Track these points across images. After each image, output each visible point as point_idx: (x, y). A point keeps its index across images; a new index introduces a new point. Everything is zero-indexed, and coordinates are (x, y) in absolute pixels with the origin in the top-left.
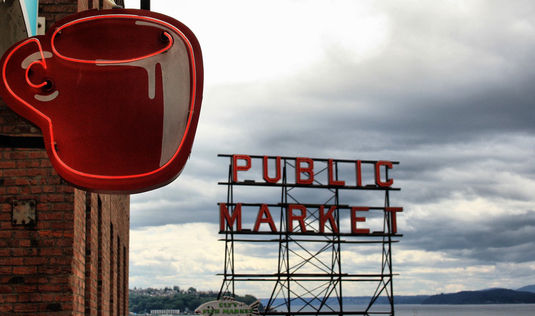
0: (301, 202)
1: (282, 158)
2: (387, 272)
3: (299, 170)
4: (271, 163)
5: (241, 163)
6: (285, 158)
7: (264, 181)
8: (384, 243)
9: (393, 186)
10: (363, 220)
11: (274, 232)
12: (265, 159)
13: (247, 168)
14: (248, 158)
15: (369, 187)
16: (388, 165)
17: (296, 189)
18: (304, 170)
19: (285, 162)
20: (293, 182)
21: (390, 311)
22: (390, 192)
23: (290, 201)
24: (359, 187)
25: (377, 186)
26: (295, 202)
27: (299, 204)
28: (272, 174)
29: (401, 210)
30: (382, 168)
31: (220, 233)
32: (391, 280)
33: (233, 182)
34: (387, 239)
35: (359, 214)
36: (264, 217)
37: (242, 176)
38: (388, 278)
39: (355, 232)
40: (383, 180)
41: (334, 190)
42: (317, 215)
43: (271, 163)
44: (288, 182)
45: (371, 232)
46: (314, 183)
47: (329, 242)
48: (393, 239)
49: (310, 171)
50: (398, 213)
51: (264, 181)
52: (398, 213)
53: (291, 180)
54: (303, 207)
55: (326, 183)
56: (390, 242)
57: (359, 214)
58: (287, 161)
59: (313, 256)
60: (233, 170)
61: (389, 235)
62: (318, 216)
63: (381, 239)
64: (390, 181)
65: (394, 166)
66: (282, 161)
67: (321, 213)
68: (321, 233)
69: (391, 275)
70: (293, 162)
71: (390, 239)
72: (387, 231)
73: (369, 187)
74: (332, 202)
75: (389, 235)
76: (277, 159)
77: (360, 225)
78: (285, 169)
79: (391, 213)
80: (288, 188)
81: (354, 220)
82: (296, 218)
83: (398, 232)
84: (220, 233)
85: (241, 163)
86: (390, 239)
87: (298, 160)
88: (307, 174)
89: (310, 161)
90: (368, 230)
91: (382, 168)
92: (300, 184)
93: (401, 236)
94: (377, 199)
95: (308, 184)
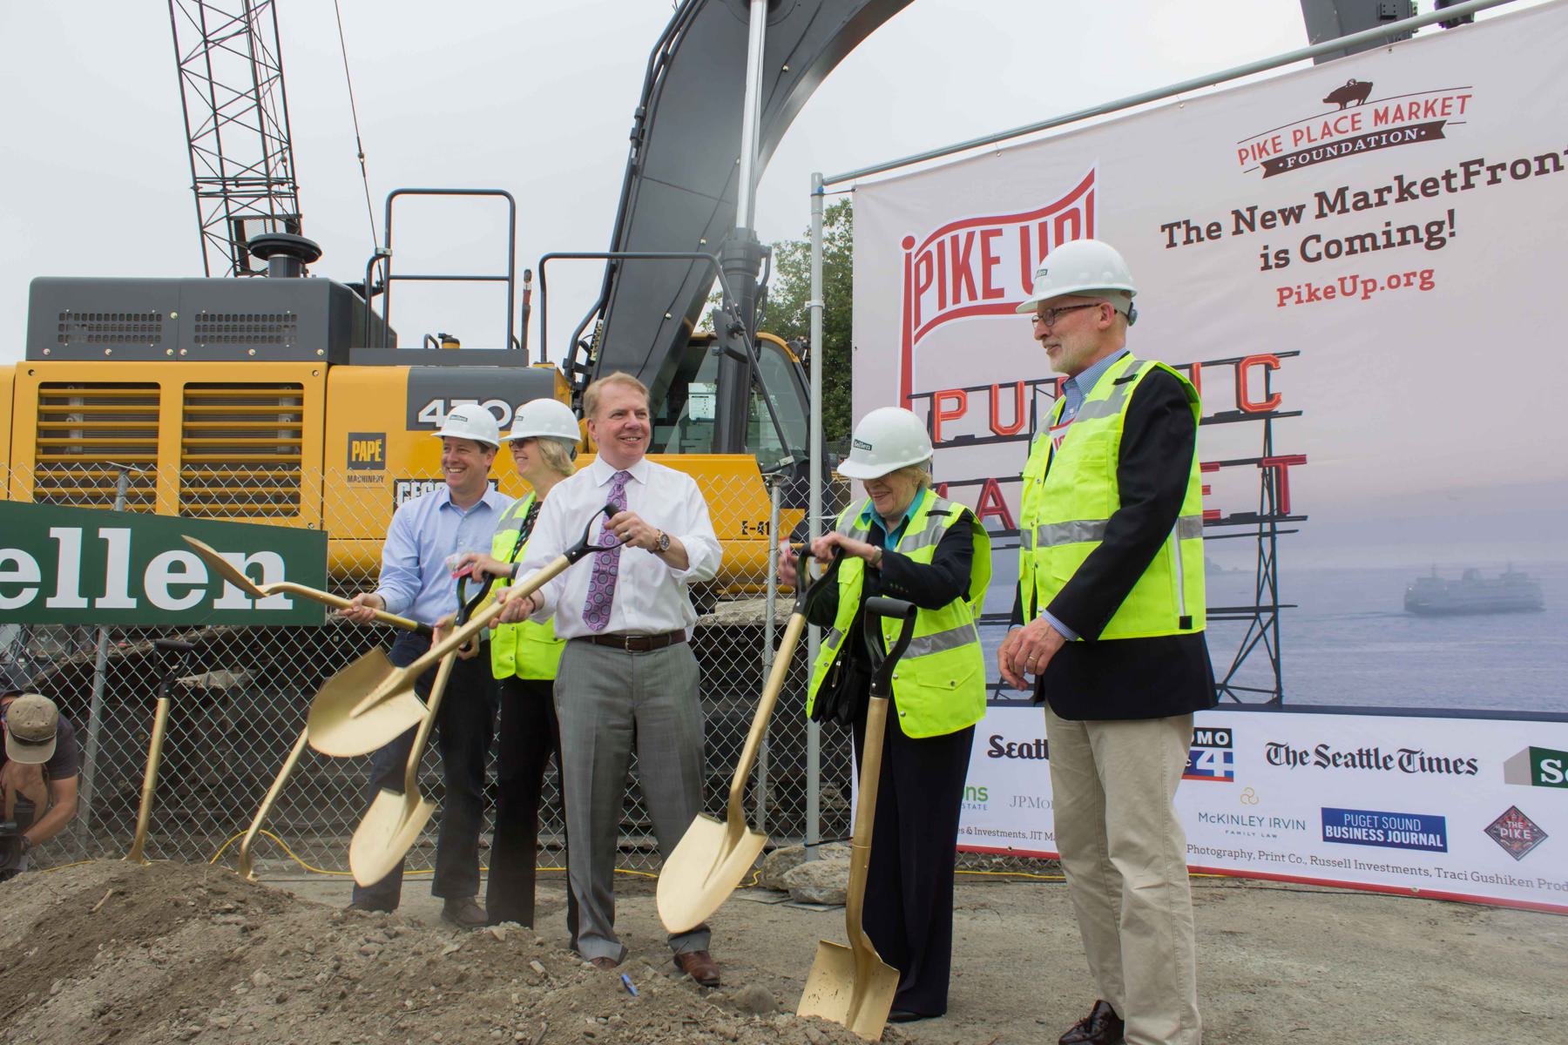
1: (1027, 383)
2: (1266, 600)
4: (1006, 398)
8: (1261, 535)
9: (1280, 409)
14: (961, 394)
16: (1270, 364)
21: (1273, 687)
28: (1006, 419)
29: (1301, 460)
30: (1255, 374)
32: (1275, 619)
34: (1267, 527)
36: (991, 503)
38: (1270, 615)
40: (1256, 396)
43: (1006, 398)
45: (1224, 515)
48: (1280, 526)
50: (1293, 471)
56: (1272, 534)
61: (1272, 519)
63: (1255, 528)
65: (1282, 361)
66: (1028, 390)
69: (1274, 609)
71: (1273, 527)
72: (1266, 511)
73: (1221, 418)
75: (1272, 519)
79: (1275, 469)
86: (1273, 527)
90: (1217, 512)
91: (1255, 374)
93: (1304, 518)
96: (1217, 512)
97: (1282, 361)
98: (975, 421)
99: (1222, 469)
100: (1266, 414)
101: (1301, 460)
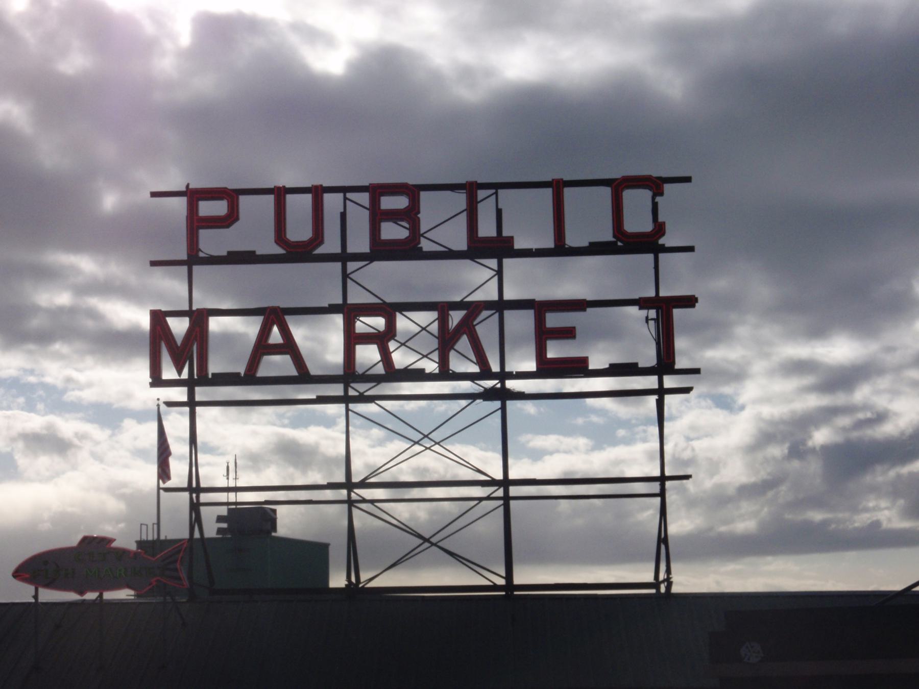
0: (388, 300)
3: (377, 216)
5: (210, 208)
6: (344, 190)
7: (279, 251)
10: (568, 333)
11: (304, 377)
12: (280, 194)
13: (230, 219)
14: (231, 196)
15: (596, 249)
16: (655, 185)
17: (376, 265)
18: (394, 216)
19: (345, 199)
20: (365, 248)
22: (662, 256)
23: (356, 297)
24: (560, 249)
25: (619, 244)
26: (378, 301)
27: (384, 302)
29: (689, 302)
31: (153, 385)
33: (194, 259)
35: (553, 320)
37: (213, 242)
39: (547, 368)
41: (493, 263)
42: (435, 328)
44: (351, 249)
46: (426, 246)
47: (488, 395)
49: (410, 215)
51: (279, 251)
52: (677, 313)
53: (360, 243)
54: (389, 310)
55: (461, 244)
57: (553, 320)
58: (349, 195)
59: (426, 436)
60: (196, 224)
62: (436, 332)
64: (660, 229)
67: (443, 320)
68: (445, 374)
70: (364, 198)
74: (490, 293)
76: (318, 192)
77: (554, 351)
78: (343, 216)
80: (352, 266)
81: (543, 335)
82: (366, 339)
83: (680, 363)
84: (153, 385)
85: (218, 208)
87: (377, 191)
88: (407, 226)
89: (413, 191)
92: (382, 251)
94: (627, 274)
95: (408, 250)
96: (584, 361)
97: (667, 187)
98: (254, 228)
99: (590, 310)
100: (649, 243)
101: (689, 302)
